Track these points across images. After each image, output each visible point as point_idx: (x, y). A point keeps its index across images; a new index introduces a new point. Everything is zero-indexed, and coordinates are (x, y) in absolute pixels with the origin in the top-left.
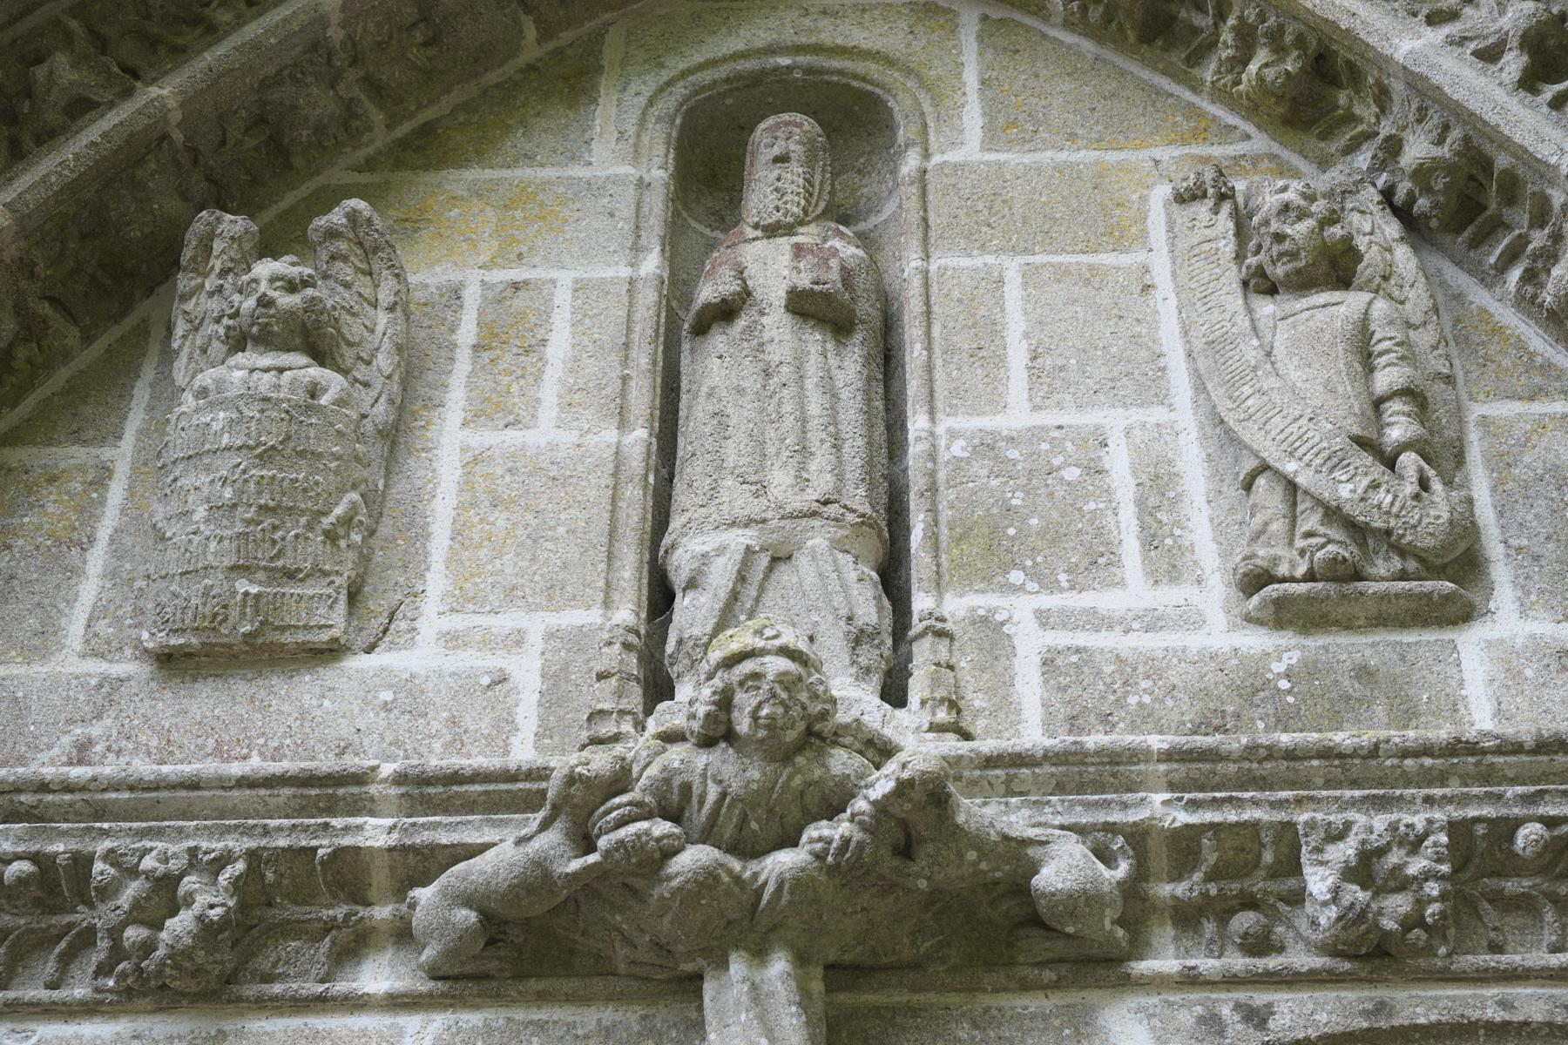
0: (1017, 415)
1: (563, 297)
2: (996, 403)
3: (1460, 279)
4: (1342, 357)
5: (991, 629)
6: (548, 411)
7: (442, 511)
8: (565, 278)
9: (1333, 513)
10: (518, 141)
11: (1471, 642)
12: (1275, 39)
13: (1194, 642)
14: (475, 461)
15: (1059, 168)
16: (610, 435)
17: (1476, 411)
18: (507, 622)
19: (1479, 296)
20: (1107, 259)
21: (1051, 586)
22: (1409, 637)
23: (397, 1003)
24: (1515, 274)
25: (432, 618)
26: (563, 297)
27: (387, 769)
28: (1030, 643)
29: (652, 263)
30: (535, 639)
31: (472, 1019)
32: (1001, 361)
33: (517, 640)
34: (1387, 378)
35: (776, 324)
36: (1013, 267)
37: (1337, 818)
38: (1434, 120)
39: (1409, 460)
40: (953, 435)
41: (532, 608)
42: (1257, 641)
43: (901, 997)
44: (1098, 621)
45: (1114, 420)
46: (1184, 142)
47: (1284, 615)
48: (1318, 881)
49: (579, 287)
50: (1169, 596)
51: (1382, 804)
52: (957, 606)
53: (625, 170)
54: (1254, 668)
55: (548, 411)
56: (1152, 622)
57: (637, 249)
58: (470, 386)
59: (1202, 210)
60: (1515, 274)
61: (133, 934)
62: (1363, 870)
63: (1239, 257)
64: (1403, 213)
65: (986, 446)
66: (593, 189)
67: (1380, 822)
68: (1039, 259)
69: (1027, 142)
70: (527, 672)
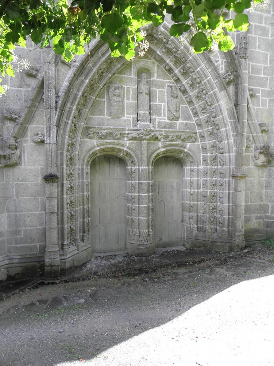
0: (157, 103)
1: (131, 89)
2: (156, 102)
3: (182, 95)
4: (176, 104)
5: (155, 119)
6: (131, 100)
7: (125, 107)
8: (131, 87)
9: (174, 115)
10: (127, 73)
11: (178, 122)
12: (176, 77)
13: (165, 121)
14: (127, 103)
15: (161, 81)
16: (135, 102)
17: (181, 105)
18: (130, 116)
19: (183, 96)
20: (163, 90)
21: (158, 116)
22: (175, 121)
23: (127, 140)
24: (185, 96)
25: (126, 115)
26: (131, 89)
27: (127, 128)
28: (157, 120)
29: (136, 87)
30: (132, 117)
31: (130, 141)
32: (156, 98)
33: (130, 117)
34: (178, 106)
35: (144, 94)
36: (157, 90)
37: (171, 135)
38: (184, 87)
39: (177, 111)
40: (154, 104)
41: (131, 115)
42: (168, 121)
43: (150, 141)
44: (160, 119)
45: (162, 104)
46: (168, 80)
47: (170, 120)
48: (170, 138)
49: (132, 88)
50: (164, 118)
51: (173, 134)
52: (154, 117)
53: (134, 77)
54: (168, 122)
55: (131, 100)
56: (163, 119)
57: (135, 85)
58: (126, 97)
59: (169, 88)
60: (185, 96)
61: (115, 137)
62: (172, 137)
63: (171, 93)
64: (180, 90)
65: (156, 105)
66: (132, 78)
67: (173, 135)
68: (159, 89)
69: (159, 78)
70: (131, 119)
